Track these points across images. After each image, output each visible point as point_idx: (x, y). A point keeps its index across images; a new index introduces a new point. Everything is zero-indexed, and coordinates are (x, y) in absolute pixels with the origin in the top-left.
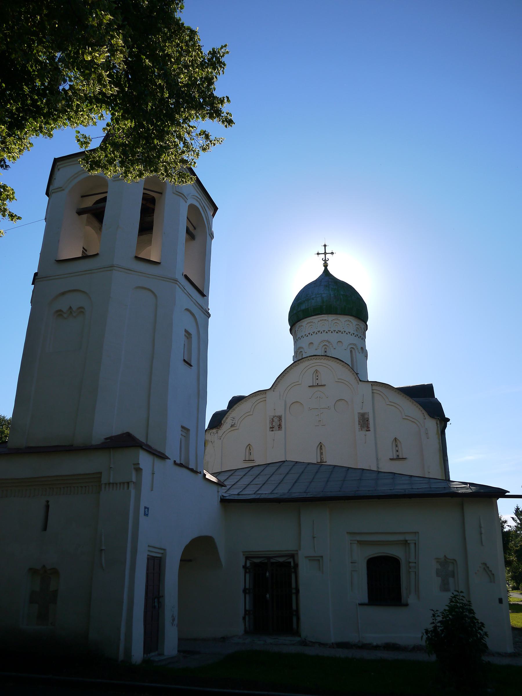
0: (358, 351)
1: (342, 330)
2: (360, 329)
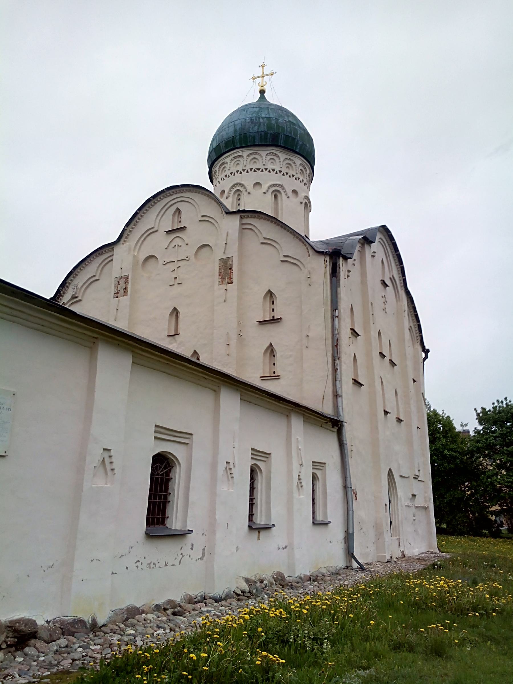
0: (286, 195)
2: (293, 165)
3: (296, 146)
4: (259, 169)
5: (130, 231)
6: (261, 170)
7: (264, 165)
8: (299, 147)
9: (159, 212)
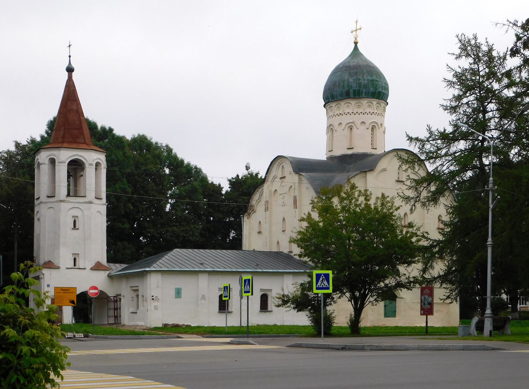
0: (356, 127)
1: (342, 113)
2: (361, 105)
3: (362, 93)
4: (340, 114)
5: (268, 177)
6: (342, 114)
7: (343, 111)
8: (364, 93)
9: (278, 165)
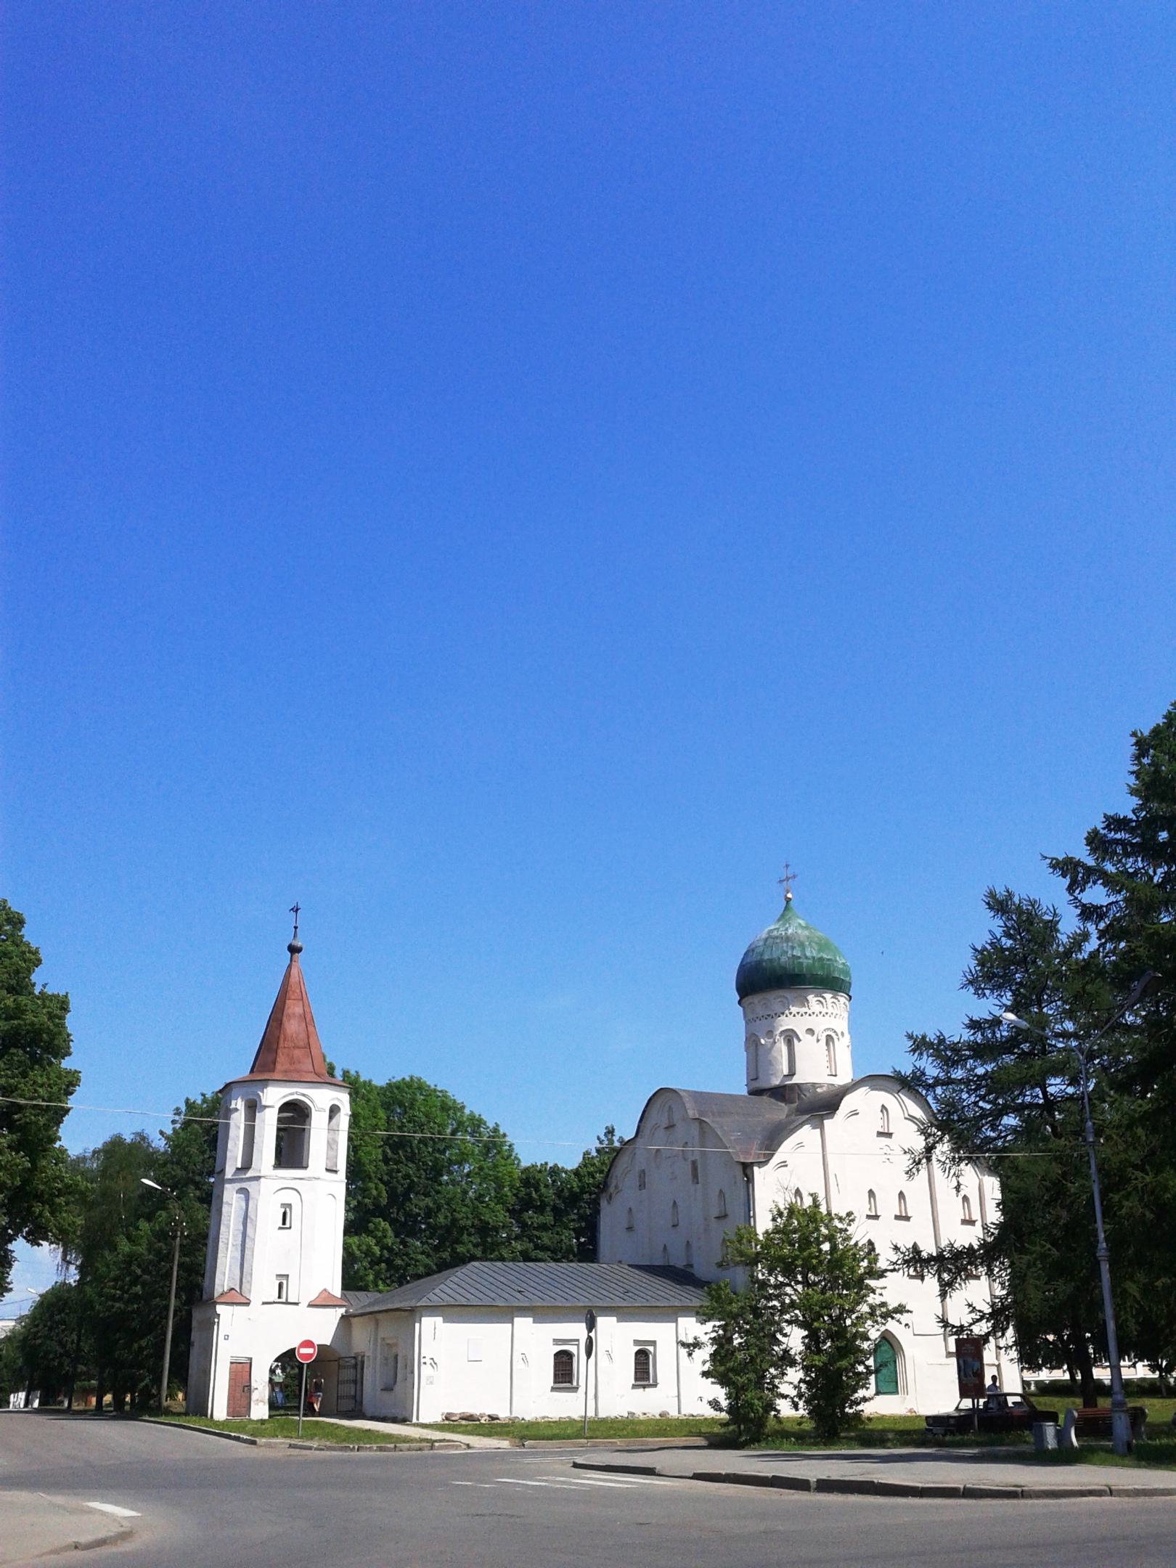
4: (769, 1015)
